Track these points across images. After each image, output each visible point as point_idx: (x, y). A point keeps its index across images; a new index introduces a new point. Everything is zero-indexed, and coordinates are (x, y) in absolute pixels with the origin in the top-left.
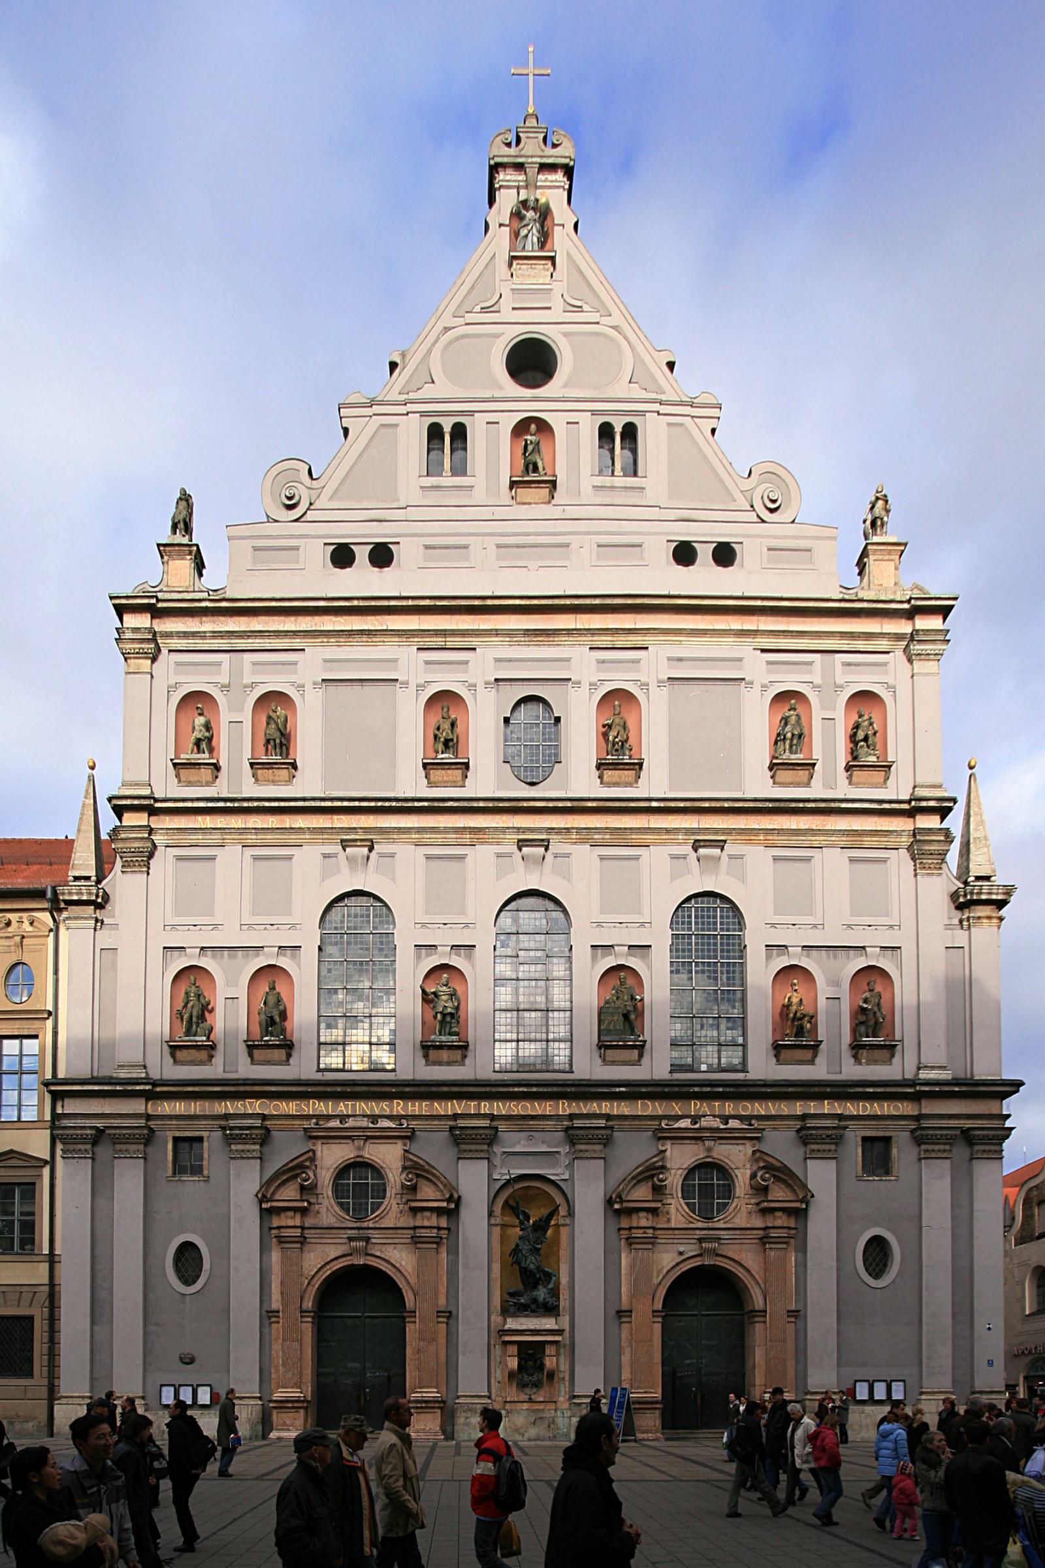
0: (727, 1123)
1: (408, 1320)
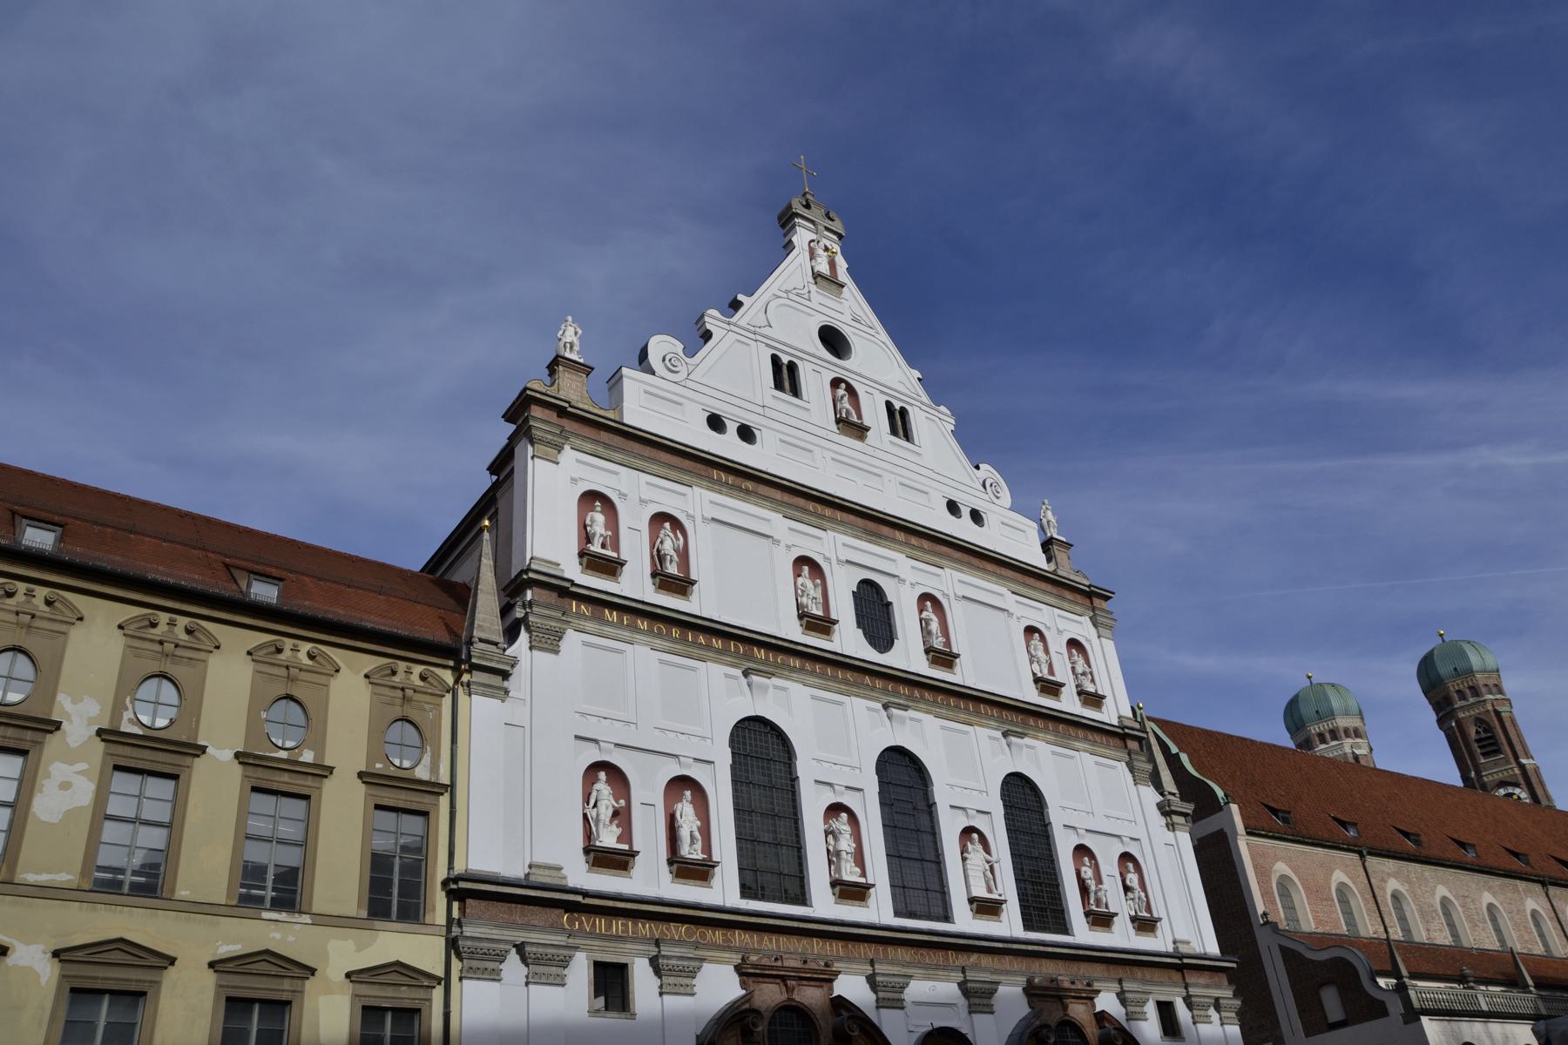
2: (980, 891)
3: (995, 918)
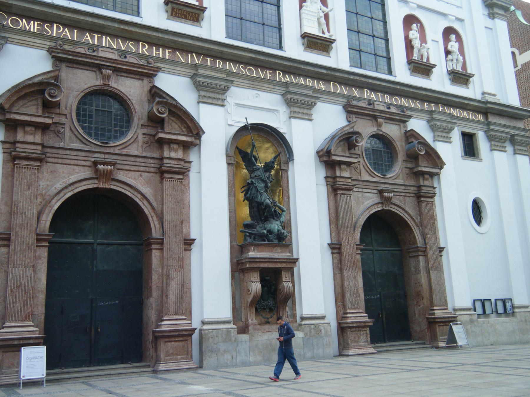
0: (389, 108)
1: (154, 246)
2: (313, 30)
3: (325, 53)
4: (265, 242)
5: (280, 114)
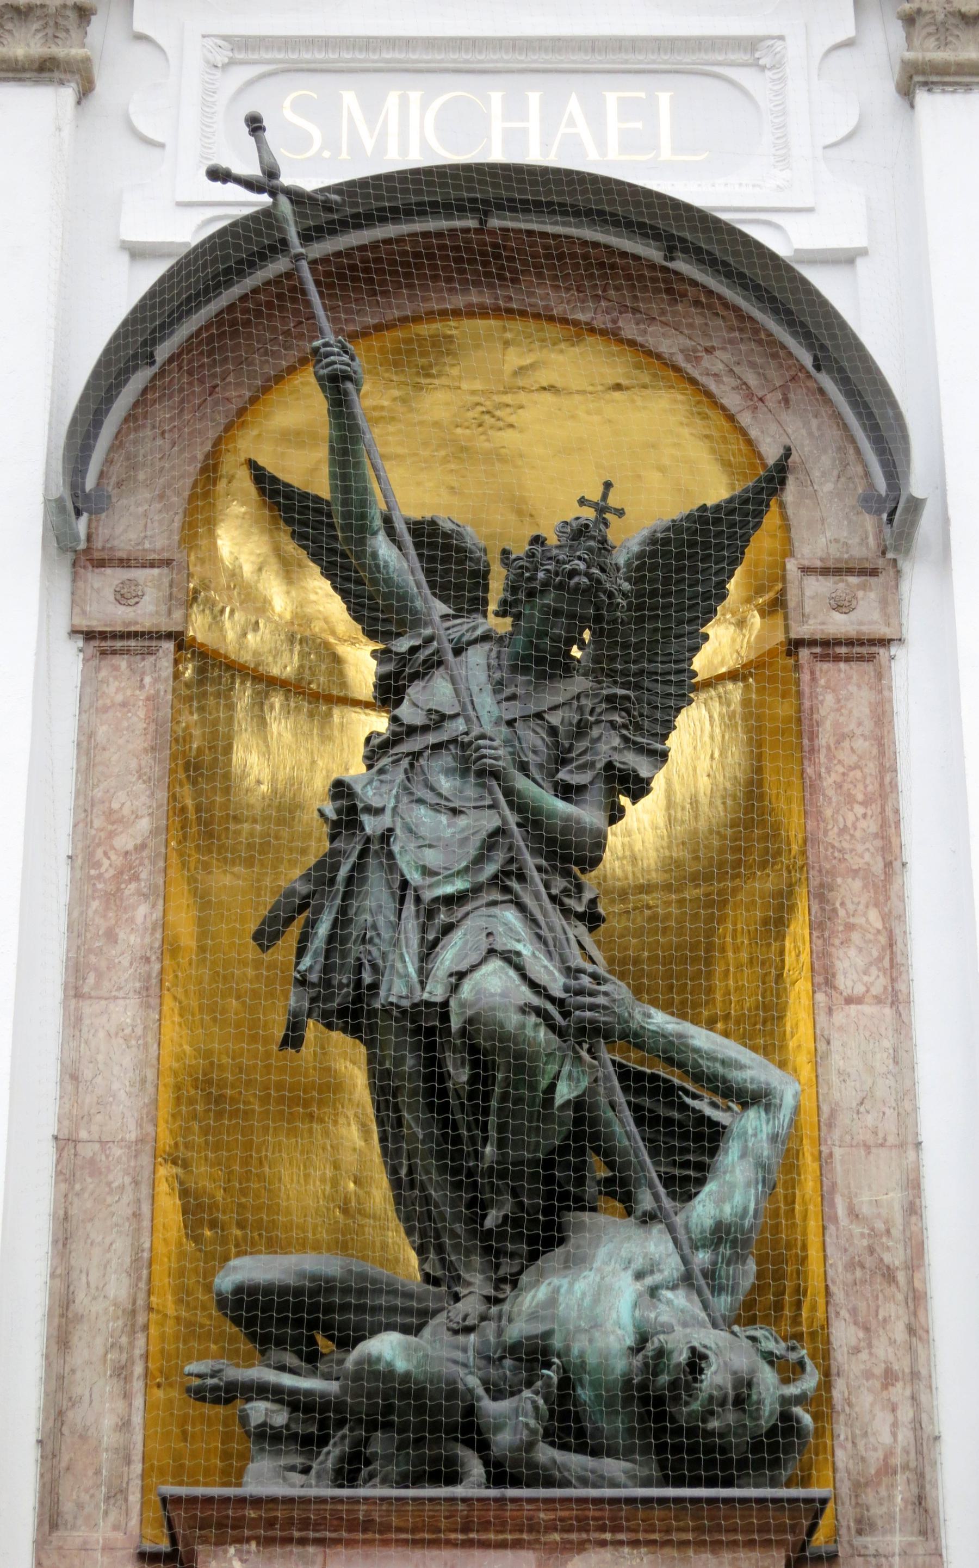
4: (458, 1491)
5: (782, 79)
